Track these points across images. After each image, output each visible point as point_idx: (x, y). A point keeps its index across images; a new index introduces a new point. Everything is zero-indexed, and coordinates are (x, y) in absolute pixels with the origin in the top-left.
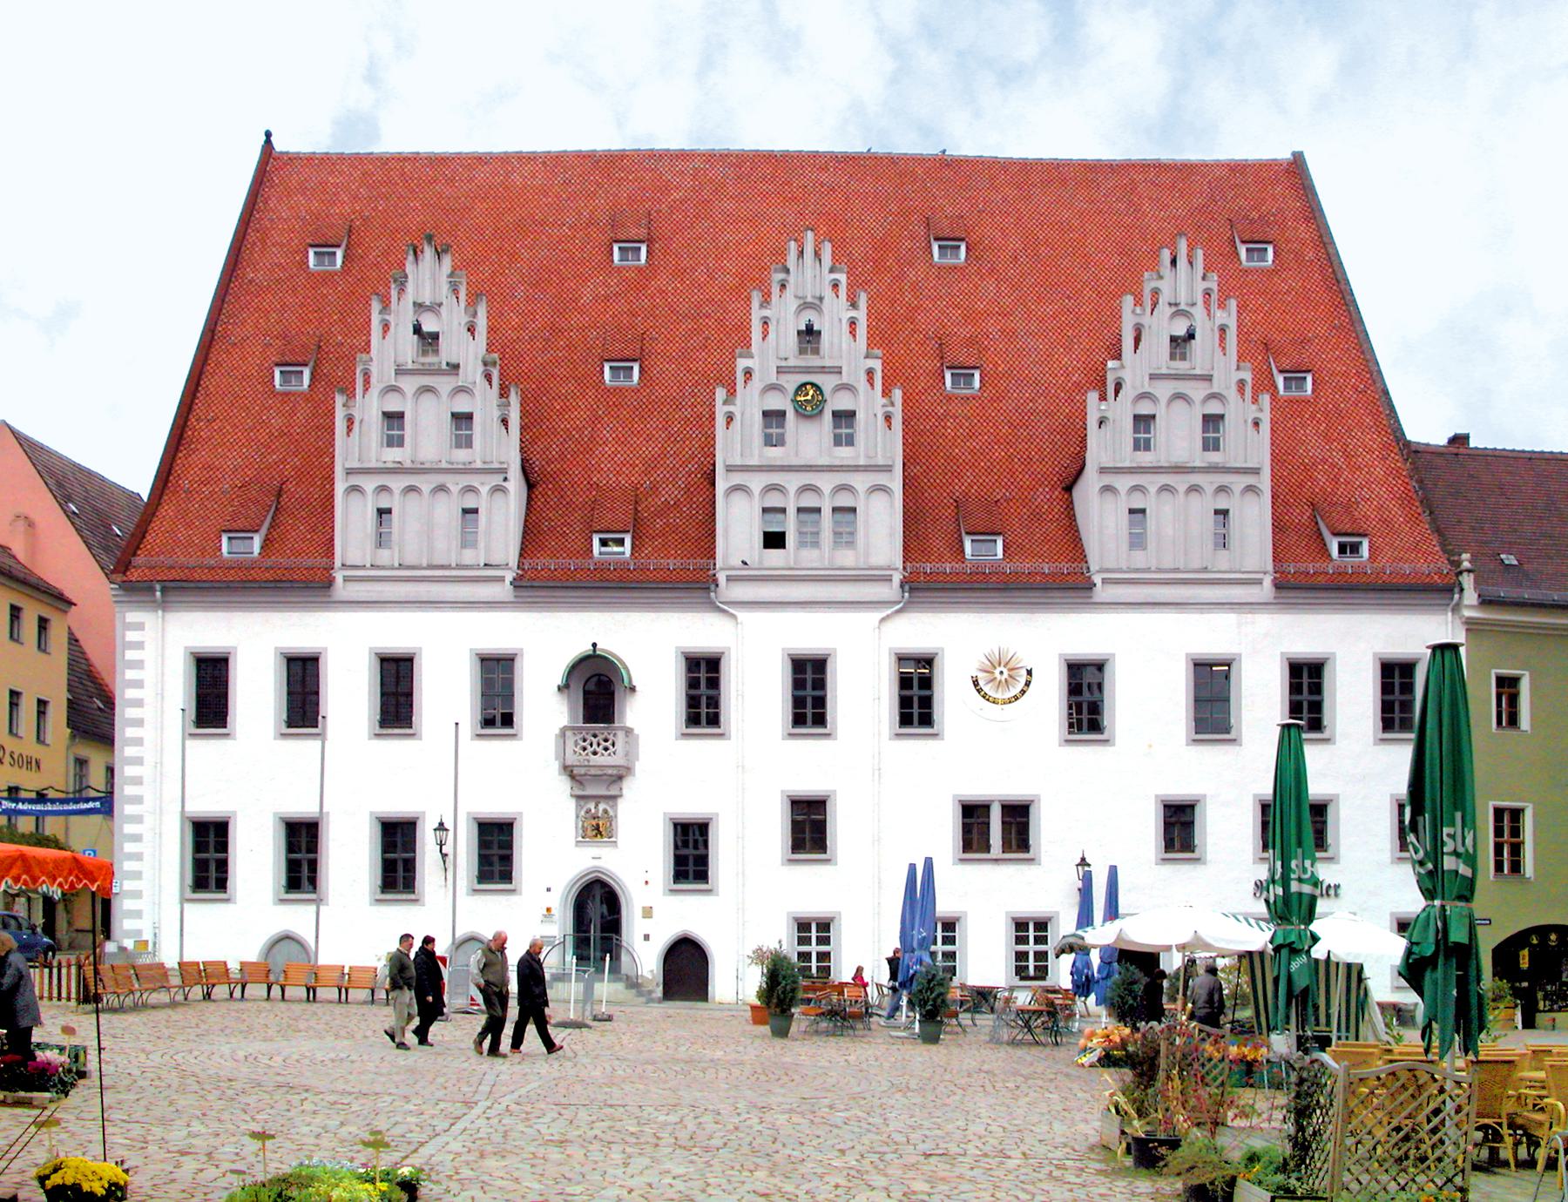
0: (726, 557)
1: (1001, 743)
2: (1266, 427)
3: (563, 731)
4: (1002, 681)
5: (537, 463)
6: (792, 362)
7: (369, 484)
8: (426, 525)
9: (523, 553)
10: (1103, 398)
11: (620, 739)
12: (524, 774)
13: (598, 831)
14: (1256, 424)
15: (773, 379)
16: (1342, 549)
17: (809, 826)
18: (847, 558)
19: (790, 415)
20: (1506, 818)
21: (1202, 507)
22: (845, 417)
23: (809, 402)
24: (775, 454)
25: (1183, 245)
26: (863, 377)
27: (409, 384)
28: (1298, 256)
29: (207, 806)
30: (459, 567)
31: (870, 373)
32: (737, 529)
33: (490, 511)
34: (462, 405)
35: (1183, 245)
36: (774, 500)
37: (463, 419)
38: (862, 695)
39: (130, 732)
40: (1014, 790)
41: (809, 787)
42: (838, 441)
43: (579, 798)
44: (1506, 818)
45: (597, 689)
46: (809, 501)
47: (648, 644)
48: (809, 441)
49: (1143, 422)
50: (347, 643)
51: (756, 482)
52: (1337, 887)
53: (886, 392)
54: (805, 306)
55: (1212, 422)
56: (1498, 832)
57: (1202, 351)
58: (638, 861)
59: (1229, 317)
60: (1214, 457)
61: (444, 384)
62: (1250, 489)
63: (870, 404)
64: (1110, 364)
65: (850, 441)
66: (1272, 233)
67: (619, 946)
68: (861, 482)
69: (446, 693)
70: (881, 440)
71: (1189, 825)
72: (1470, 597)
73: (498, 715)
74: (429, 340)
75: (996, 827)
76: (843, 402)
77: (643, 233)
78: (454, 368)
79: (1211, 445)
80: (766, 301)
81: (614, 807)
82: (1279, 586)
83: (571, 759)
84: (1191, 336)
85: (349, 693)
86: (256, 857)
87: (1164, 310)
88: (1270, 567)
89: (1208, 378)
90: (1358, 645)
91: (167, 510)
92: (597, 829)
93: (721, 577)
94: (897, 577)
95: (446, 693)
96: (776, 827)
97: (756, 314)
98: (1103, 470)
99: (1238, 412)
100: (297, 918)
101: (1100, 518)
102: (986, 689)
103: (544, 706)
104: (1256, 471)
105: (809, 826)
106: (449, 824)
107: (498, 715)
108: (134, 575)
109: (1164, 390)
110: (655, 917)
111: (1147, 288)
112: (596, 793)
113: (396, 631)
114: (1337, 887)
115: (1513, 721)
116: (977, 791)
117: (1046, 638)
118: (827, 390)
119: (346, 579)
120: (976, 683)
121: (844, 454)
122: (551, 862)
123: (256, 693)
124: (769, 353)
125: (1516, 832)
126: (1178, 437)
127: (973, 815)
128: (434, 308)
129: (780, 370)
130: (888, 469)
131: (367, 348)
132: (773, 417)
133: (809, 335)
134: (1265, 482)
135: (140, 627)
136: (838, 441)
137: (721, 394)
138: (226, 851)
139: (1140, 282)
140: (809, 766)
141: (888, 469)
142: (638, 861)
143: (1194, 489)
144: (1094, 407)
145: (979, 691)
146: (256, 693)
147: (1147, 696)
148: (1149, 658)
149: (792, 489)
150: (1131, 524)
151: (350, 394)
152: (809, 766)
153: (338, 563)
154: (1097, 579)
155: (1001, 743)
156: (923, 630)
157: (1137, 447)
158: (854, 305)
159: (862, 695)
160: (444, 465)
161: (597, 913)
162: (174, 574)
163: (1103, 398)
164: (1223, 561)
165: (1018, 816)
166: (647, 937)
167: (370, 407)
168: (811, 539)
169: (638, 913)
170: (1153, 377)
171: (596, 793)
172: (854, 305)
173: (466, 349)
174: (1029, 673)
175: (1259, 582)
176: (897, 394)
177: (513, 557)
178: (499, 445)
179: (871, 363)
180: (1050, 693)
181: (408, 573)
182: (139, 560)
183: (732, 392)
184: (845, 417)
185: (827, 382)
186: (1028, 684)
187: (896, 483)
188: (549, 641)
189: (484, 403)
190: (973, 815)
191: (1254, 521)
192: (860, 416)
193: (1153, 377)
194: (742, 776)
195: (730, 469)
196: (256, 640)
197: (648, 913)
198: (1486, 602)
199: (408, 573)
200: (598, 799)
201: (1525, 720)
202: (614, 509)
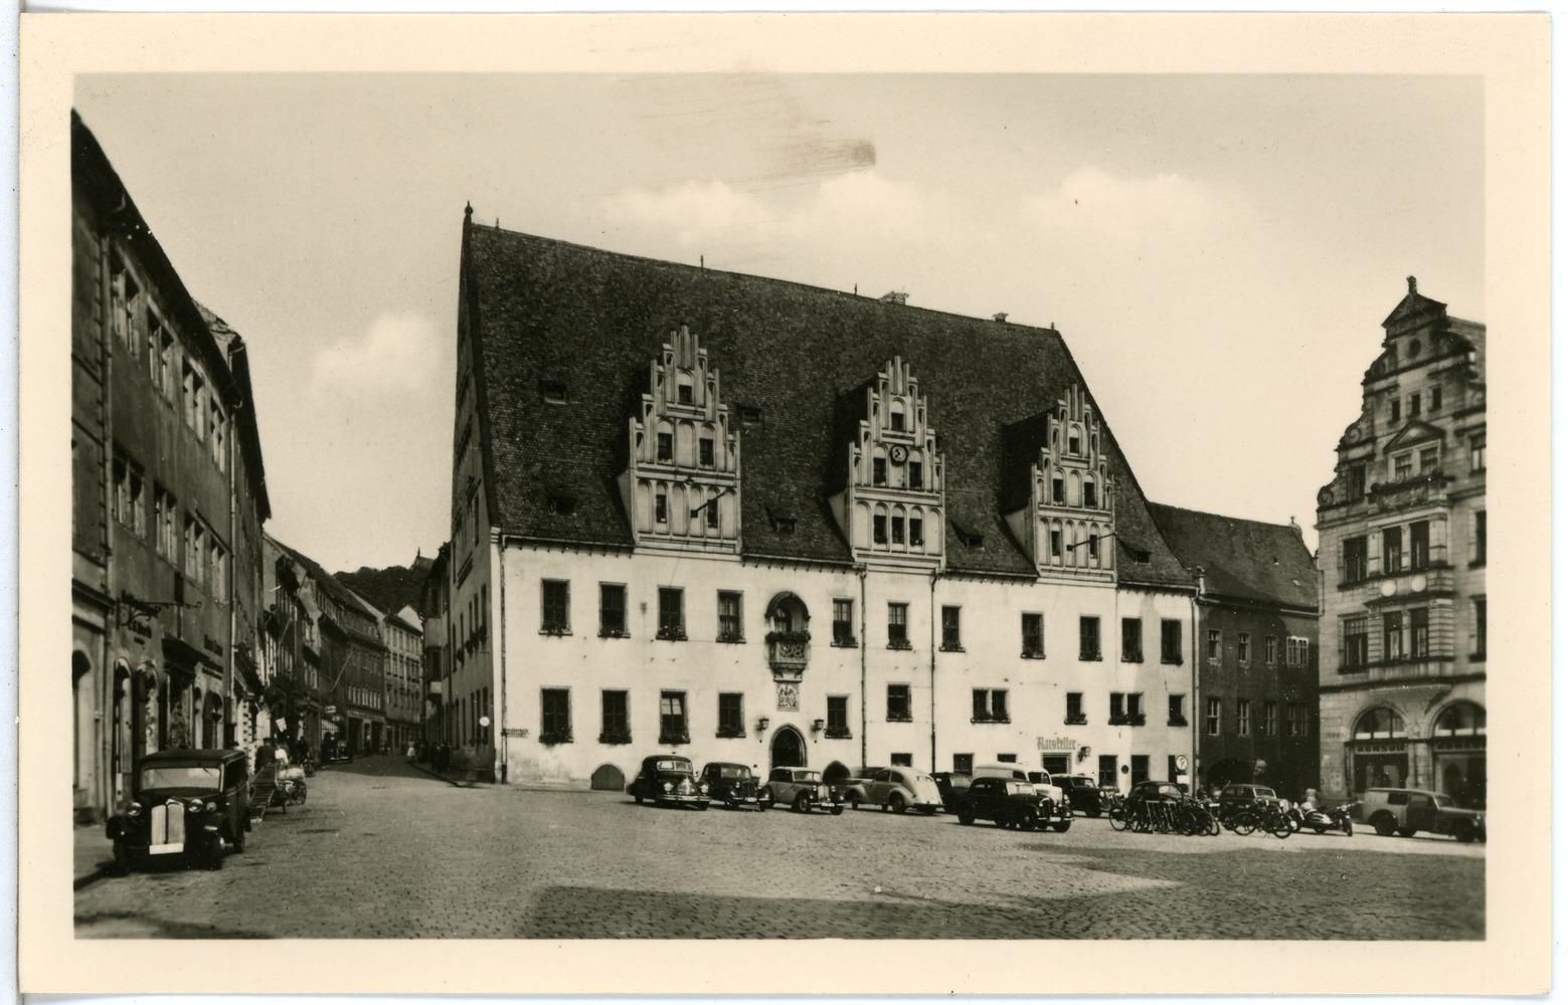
12: (746, 668)
17: (899, 703)
22: (916, 468)
38: (923, 629)
40: (999, 685)
46: (899, 513)
63: (928, 460)
69: (701, 615)
73: (731, 633)
76: (915, 457)
81: (796, 688)
92: (787, 702)
96: (879, 704)
103: (756, 625)
105: (899, 703)
107: (731, 633)
110: (820, 753)
116: (981, 685)
123: (584, 609)
132: (879, 464)
146: (584, 609)
147: (1061, 637)
156: (951, 591)
159: (923, 629)
168: (899, 538)
183: (858, 445)
188: (758, 585)
196: (585, 574)
202: (797, 512)
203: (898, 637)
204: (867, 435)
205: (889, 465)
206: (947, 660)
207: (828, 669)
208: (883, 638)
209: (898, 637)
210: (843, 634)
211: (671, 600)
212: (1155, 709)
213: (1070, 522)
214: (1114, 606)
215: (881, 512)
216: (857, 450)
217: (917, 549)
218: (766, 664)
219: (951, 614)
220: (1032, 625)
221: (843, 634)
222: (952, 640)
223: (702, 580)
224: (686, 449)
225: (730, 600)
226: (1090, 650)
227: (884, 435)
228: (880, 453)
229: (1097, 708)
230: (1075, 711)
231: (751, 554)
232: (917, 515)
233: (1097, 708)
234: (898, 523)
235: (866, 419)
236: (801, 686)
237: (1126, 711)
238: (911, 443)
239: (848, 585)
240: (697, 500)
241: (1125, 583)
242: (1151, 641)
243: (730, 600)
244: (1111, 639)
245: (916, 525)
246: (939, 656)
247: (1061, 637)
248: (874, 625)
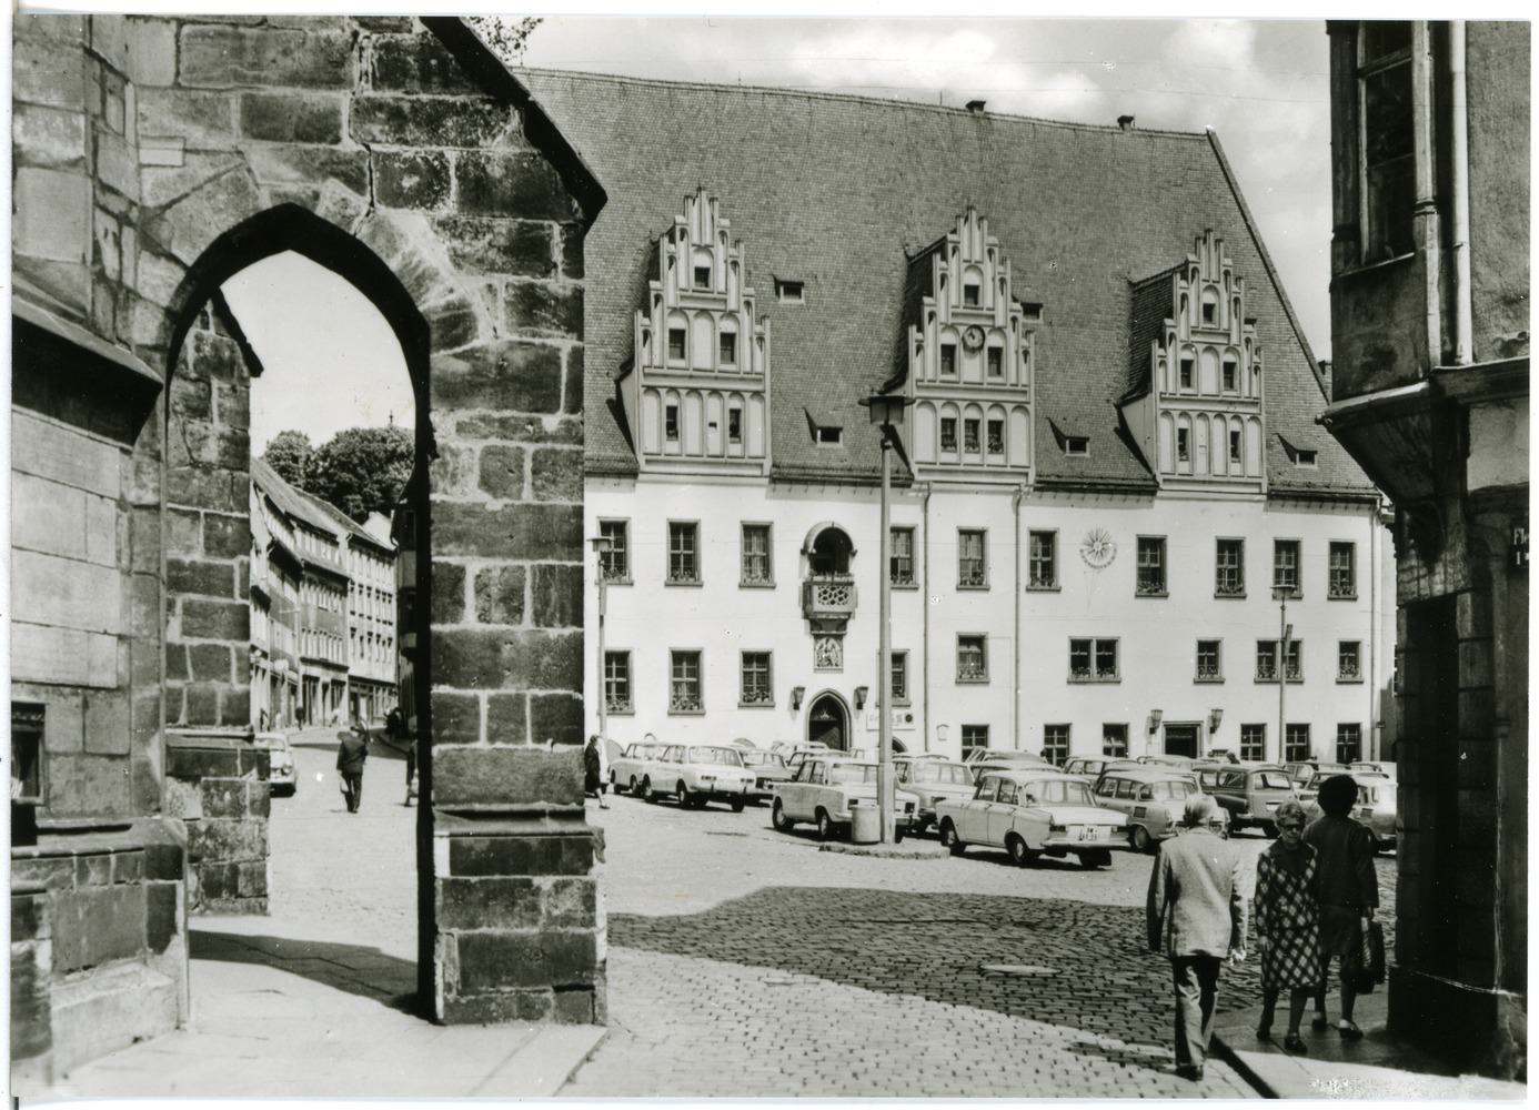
6: (961, 310)
22: (996, 354)
38: (1007, 560)
40: (1106, 633)
45: (830, 551)
46: (973, 414)
69: (720, 553)
75: (1094, 659)
76: (994, 340)
96: (946, 653)
103: (790, 567)
112: (827, 629)
113: (685, 501)
117: (1124, 523)
126: (1208, 377)
127: (1079, 646)
132: (948, 352)
140: (974, 613)
144: (1157, 351)
147: (1192, 567)
152: (974, 613)
155: (1098, 593)
156: (1043, 514)
165: (1108, 647)
168: (973, 444)
171: (827, 629)
183: (920, 329)
184: (996, 354)
186: (1113, 558)
190: (1079, 646)
194: (929, 619)
203: (974, 576)
204: (932, 315)
205: (960, 352)
206: (1038, 604)
208: (953, 575)
209: (974, 576)
210: (901, 572)
211: (683, 534)
212: (1320, 660)
213: (1202, 415)
214: (1260, 529)
215: (949, 413)
216: (920, 336)
217: (997, 459)
219: (1045, 540)
220: (1152, 548)
221: (901, 572)
223: (720, 515)
225: (757, 534)
226: (1230, 581)
227: (954, 315)
228: (949, 338)
229: (1239, 660)
230: (1209, 655)
231: (786, 477)
232: (996, 415)
233: (1239, 660)
234: (973, 425)
235: (930, 294)
236: (846, 640)
237: (1278, 659)
238: (990, 323)
239: (904, 512)
240: (716, 409)
241: (1280, 496)
242: (1315, 569)
243: (757, 534)
244: (1259, 567)
245: (996, 427)
246: (1025, 597)
247: (1192, 567)
248: (941, 558)
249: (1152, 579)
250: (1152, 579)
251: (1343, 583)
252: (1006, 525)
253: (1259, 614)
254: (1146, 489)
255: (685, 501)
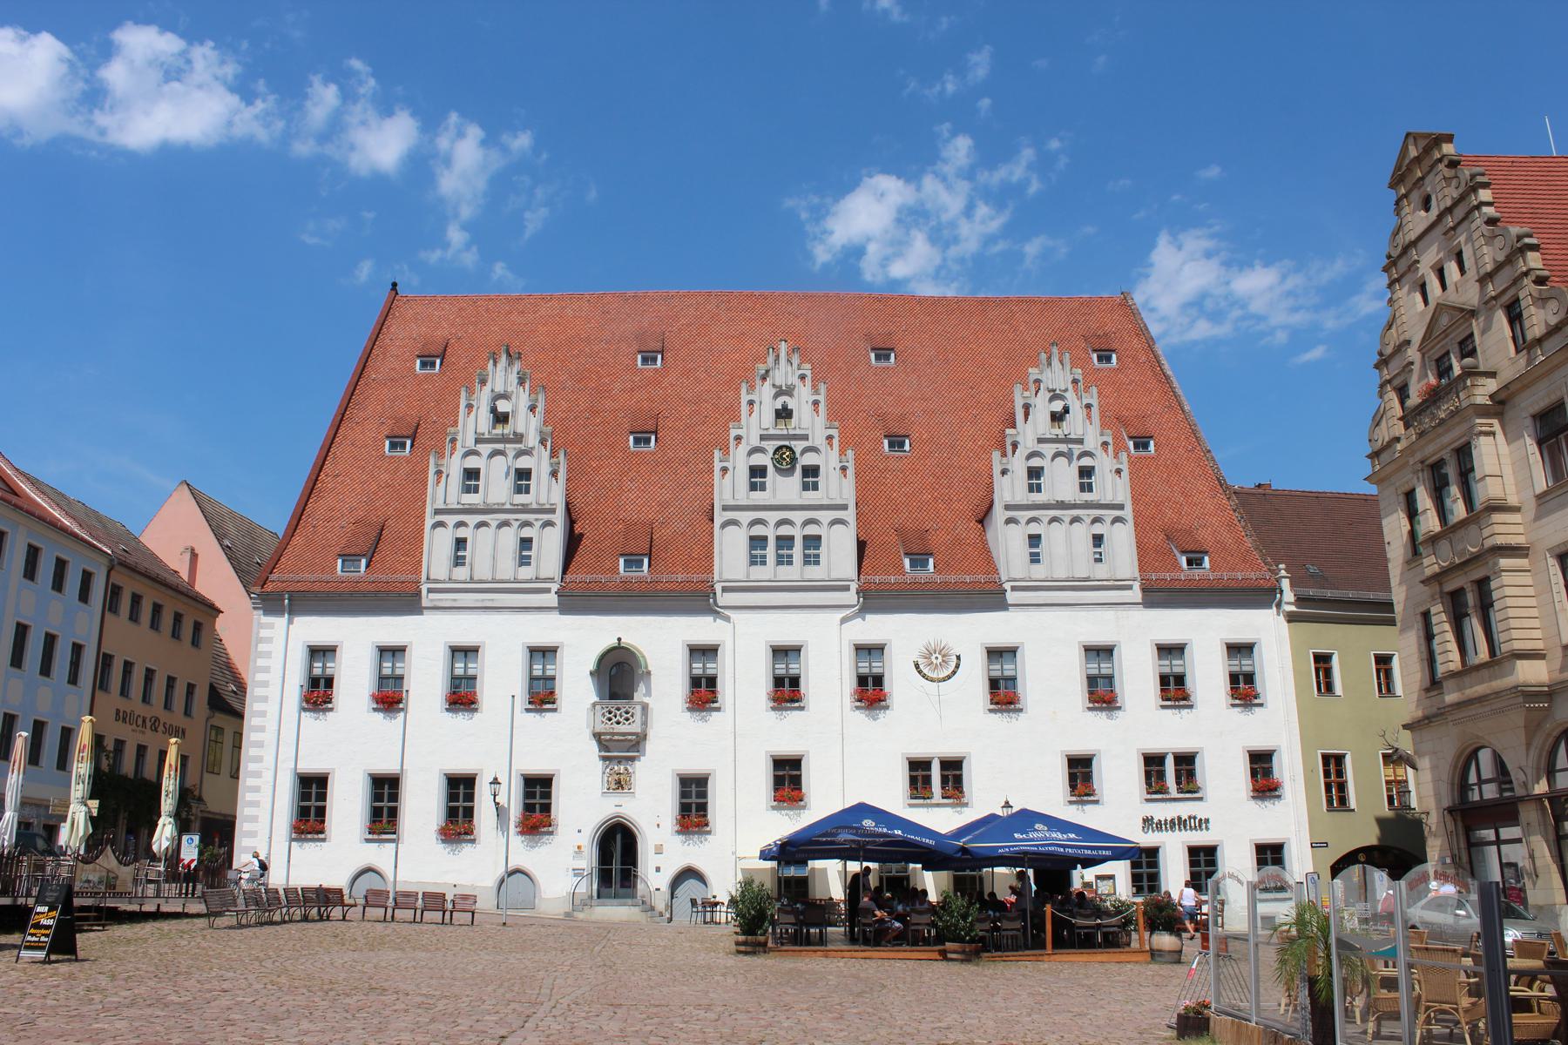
0: (720, 574)
1: (937, 713)
2: (1125, 474)
3: (594, 705)
4: (937, 666)
5: (578, 503)
6: (772, 432)
7: (451, 520)
8: (492, 550)
9: (565, 570)
10: (1004, 455)
11: (638, 710)
13: (619, 785)
14: (1118, 471)
15: (755, 442)
16: (1190, 562)
18: (813, 572)
19: (770, 470)
20: (1332, 761)
21: (1083, 533)
22: (811, 471)
23: (785, 459)
24: (758, 497)
25: (1055, 350)
26: (825, 442)
27: (486, 449)
28: (1135, 358)
29: (310, 766)
30: (516, 581)
31: (830, 438)
32: (730, 554)
33: (540, 538)
34: (523, 463)
35: (1055, 350)
36: (758, 530)
37: (523, 474)
39: (257, 707)
40: (950, 750)
41: (787, 749)
42: (806, 487)
43: (604, 759)
44: (1332, 761)
45: (618, 674)
46: (785, 530)
47: (661, 641)
48: (785, 488)
49: (1034, 473)
50: (426, 638)
51: (745, 517)
52: (1207, 821)
53: (842, 452)
54: (780, 392)
55: (1086, 472)
56: (1327, 774)
57: (1075, 424)
58: (651, 809)
59: (1093, 398)
60: (1087, 497)
61: (511, 449)
62: (1117, 520)
63: (828, 460)
64: (1009, 431)
65: (815, 487)
66: (1114, 346)
67: (636, 876)
68: (825, 516)
69: (502, 680)
70: (838, 486)
71: (1088, 777)
72: (1289, 595)
73: (542, 696)
74: (501, 418)
76: (809, 459)
77: (658, 346)
78: (519, 438)
79: (1086, 488)
80: (751, 388)
82: (1145, 590)
83: (600, 728)
84: (1066, 410)
85: (426, 681)
86: (348, 805)
87: (1044, 395)
88: (1137, 574)
89: (1080, 441)
90: (1206, 632)
91: (297, 540)
93: (718, 587)
94: (854, 586)
95: (502, 680)
97: (745, 398)
98: (1008, 507)
99: (1104, 464)
100: (379, 855)
101: (1008, 543)
102: (925, 671)
103: (577, 686)
104: (1121, 507)
106: (503, 779)
107: (542, 696)
108: (269, 587)
109: (1049, 449)
110: (662, 853)
111: (1032, 378)
113: (464, 628)
114: (1207, 821)
115: (1329, 688)
116: (920, 751)
117: (969, 633)
118: (798, 451)
119: (430, 591)
120: (917, 666)
121: (811, 497)
122: (581, 810)
123: (355, 679)
124: (756, 421)
125: (1340, 773)
128: (505, 396)
129: (763, 438)
130: (844, 507)
131: (455, 423)
132: (757, 472)
133: (784, 414)
134: (1128, 513)
135: (271, 626)
136: (806, 487)
137: (717, 454)
138: (325, 800)
139: (1027, 375)
141: (844, 507)
142: (651, 809)
143: (1075, 520)
145: (920, 672)
147: (1051, 676)
148: (1050, 644)
149: (772, 523)
150: (1031, 546)
151: (441, 455)
153: (424, 578)
154: (1007, 586)
156: (875, 627)
157: (1031, 489)
158: (817, 392)
160: (508, 506)
161: (617, 850)
162: (299, 587)
163: (1004, 455)
164: (1101, 571)
166: (658, 869)
167: (455, 466)
169: (652, 850)
170: (1040, 441)
172: (817, 392)
173: (528, 424)
174: (958, 658)
175: (1130, 588)
176: (850, 453)
177: (558, 576)
178: (549, 491)
179: (831, 432)
180: (975, 674)
181: (475, 586)
182: (273, 577)
184: (811, 471)
185: (798, 446)
186: (957, 666)
187: (850, 515)
188: (584, 639)
189: (539, 463)
191: (1122, 540)
192: (822, 470)
193: (1040, 441)
194: (735, 744)
195: (725, 508)
196: (356, 638)
197: (659, 850)
198: (1300, 601)
199: (475, 586)
200: (620, 760)
201: (1338, 688)
203: (787, 691)
207: (674, 739)
209: (787, 691)
210: (703, 692)
214: (1138, 632)
217: (813, 572)
218: (587, 734)
221: (703, 692)
222: (870, 691)
224: (496, 486)
226: (1102, 694)
237: (1170, 773)
242: (1208, 675)
244: (1137, 676)
245: (813, 541)
247: (1051, 676)
248: (745, 678)
249: (1003, 694)
250: (1003, 694)
251: (1243, 688)
252: (828, 644)
253: (1145, 724)
254: (990, 597)
255: (464, 628)
